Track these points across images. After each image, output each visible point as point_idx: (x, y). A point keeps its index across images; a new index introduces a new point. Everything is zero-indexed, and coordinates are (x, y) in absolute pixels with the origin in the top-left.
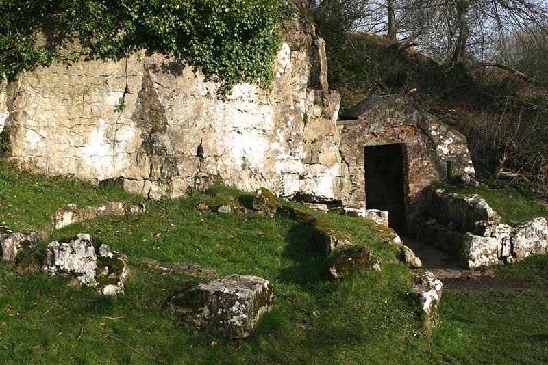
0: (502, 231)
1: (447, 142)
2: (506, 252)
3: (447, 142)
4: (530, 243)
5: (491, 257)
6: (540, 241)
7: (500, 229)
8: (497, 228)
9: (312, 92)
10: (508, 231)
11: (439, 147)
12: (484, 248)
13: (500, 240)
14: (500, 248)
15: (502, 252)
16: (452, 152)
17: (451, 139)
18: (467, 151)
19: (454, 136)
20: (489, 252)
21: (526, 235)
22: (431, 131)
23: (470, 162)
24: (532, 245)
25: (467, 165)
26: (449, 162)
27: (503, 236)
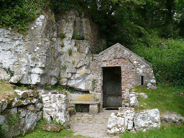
0: (129, 114)
1: (142, 67)
2: (130, 127)
3: (142, 67)
4: (146, 124)
5: (120, 129)
6: (153, 123)
7: (127, 113)
8: (126, 112)
9: (73, 41)
10: (133, 115)
11: (138, 69)
12: (116, 123)
13: (127, 120)
14: (126, 124)
15: (127, 127)
16: (144, 72)
17: (144, 65)
18: (152, 71)
19: (146, 64)
20: (119, 126)
21: (143, 118)
22: (133, 61)
23: (154, 77)
24: (147, 125)
25: (152, 79)
26: (142, 77)
27: (129, 117)
